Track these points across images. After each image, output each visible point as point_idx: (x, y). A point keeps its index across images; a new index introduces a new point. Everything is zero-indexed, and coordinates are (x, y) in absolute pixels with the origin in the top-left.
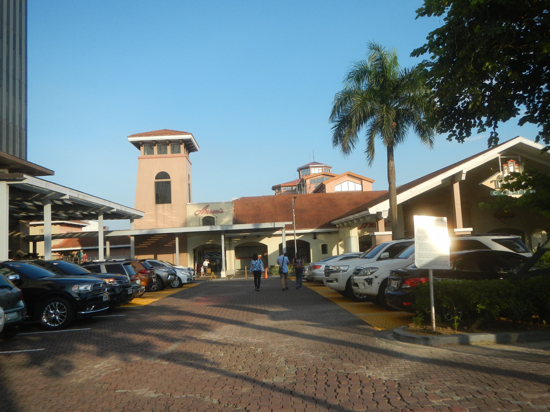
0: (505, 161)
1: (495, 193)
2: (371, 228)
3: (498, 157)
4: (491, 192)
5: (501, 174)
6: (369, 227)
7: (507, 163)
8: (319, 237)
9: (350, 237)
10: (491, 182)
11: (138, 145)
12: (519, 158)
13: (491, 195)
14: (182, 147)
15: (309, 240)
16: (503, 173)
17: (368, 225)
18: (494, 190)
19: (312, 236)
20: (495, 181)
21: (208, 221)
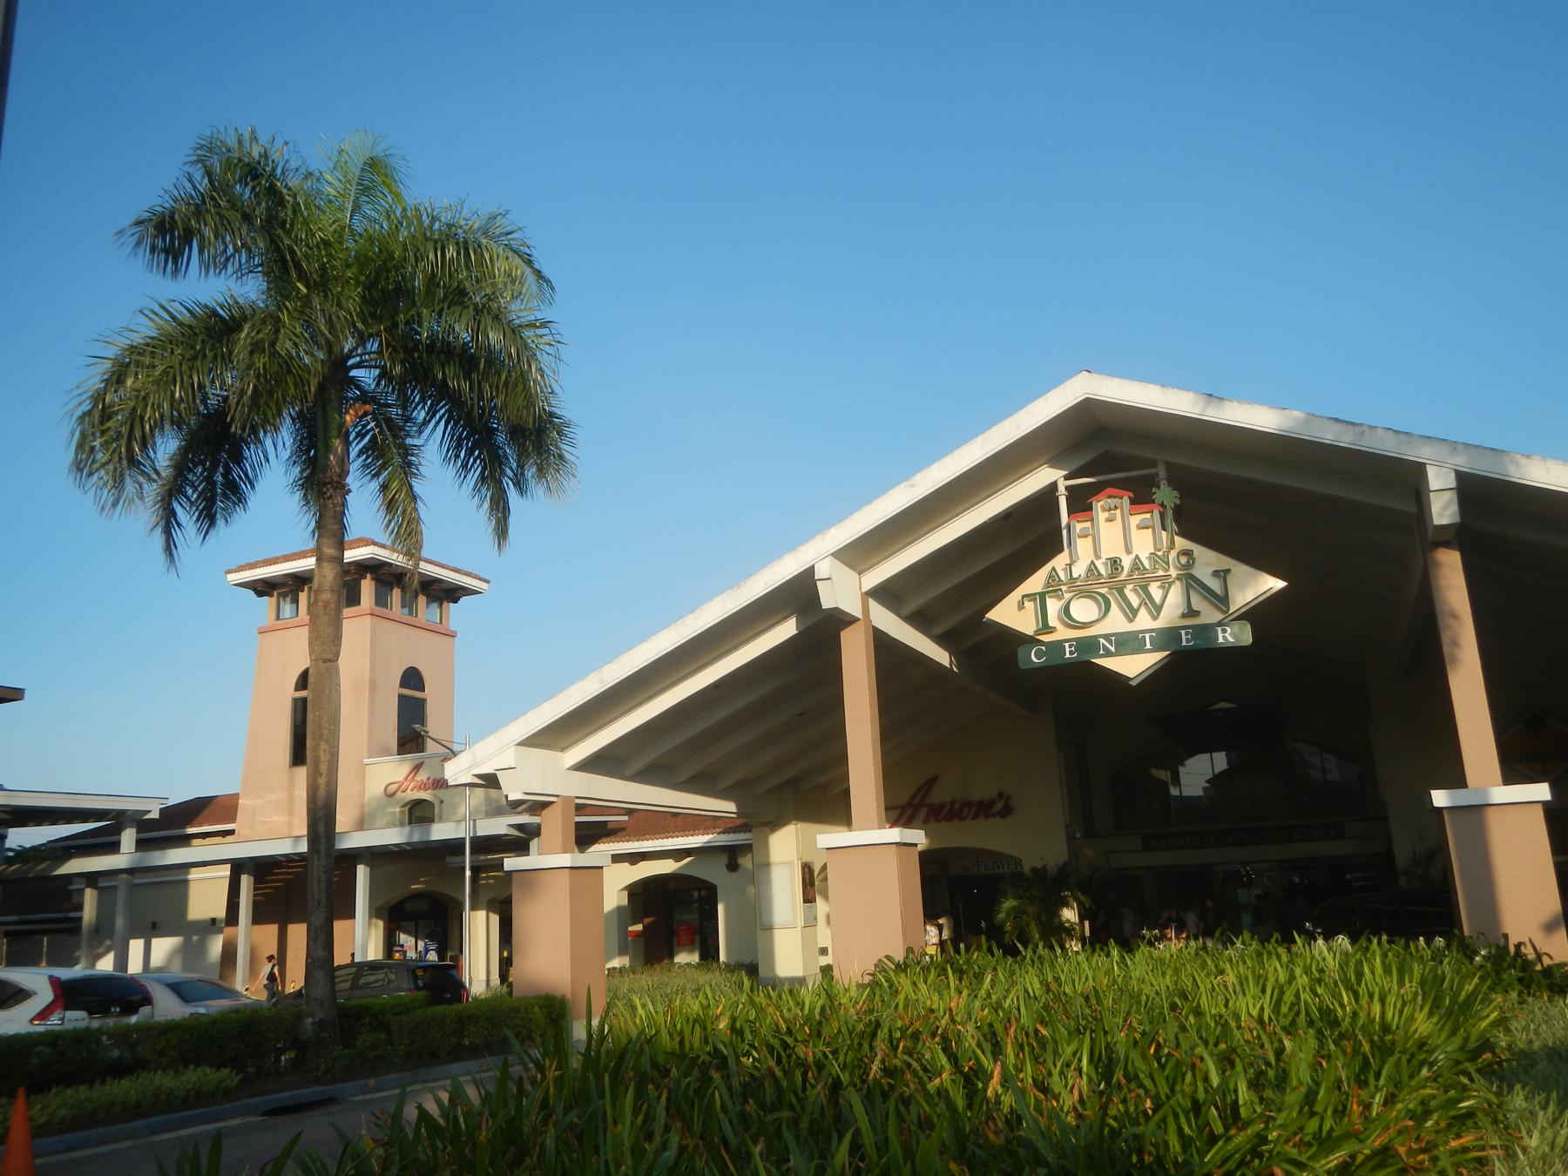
0: (1081, 502)
2: (933, 824)
4: (1021, 651)
5: (1059, 562)
8: (745, 862)
9: (767, 865)
10: (1021, 606)
11: (263, 588)
13: (1023, 666)
14: (367, 587)
15: (713, 872)
17: (923, 812)
18: (1031, 641)
19: (723, 860)
21: (419, 813)
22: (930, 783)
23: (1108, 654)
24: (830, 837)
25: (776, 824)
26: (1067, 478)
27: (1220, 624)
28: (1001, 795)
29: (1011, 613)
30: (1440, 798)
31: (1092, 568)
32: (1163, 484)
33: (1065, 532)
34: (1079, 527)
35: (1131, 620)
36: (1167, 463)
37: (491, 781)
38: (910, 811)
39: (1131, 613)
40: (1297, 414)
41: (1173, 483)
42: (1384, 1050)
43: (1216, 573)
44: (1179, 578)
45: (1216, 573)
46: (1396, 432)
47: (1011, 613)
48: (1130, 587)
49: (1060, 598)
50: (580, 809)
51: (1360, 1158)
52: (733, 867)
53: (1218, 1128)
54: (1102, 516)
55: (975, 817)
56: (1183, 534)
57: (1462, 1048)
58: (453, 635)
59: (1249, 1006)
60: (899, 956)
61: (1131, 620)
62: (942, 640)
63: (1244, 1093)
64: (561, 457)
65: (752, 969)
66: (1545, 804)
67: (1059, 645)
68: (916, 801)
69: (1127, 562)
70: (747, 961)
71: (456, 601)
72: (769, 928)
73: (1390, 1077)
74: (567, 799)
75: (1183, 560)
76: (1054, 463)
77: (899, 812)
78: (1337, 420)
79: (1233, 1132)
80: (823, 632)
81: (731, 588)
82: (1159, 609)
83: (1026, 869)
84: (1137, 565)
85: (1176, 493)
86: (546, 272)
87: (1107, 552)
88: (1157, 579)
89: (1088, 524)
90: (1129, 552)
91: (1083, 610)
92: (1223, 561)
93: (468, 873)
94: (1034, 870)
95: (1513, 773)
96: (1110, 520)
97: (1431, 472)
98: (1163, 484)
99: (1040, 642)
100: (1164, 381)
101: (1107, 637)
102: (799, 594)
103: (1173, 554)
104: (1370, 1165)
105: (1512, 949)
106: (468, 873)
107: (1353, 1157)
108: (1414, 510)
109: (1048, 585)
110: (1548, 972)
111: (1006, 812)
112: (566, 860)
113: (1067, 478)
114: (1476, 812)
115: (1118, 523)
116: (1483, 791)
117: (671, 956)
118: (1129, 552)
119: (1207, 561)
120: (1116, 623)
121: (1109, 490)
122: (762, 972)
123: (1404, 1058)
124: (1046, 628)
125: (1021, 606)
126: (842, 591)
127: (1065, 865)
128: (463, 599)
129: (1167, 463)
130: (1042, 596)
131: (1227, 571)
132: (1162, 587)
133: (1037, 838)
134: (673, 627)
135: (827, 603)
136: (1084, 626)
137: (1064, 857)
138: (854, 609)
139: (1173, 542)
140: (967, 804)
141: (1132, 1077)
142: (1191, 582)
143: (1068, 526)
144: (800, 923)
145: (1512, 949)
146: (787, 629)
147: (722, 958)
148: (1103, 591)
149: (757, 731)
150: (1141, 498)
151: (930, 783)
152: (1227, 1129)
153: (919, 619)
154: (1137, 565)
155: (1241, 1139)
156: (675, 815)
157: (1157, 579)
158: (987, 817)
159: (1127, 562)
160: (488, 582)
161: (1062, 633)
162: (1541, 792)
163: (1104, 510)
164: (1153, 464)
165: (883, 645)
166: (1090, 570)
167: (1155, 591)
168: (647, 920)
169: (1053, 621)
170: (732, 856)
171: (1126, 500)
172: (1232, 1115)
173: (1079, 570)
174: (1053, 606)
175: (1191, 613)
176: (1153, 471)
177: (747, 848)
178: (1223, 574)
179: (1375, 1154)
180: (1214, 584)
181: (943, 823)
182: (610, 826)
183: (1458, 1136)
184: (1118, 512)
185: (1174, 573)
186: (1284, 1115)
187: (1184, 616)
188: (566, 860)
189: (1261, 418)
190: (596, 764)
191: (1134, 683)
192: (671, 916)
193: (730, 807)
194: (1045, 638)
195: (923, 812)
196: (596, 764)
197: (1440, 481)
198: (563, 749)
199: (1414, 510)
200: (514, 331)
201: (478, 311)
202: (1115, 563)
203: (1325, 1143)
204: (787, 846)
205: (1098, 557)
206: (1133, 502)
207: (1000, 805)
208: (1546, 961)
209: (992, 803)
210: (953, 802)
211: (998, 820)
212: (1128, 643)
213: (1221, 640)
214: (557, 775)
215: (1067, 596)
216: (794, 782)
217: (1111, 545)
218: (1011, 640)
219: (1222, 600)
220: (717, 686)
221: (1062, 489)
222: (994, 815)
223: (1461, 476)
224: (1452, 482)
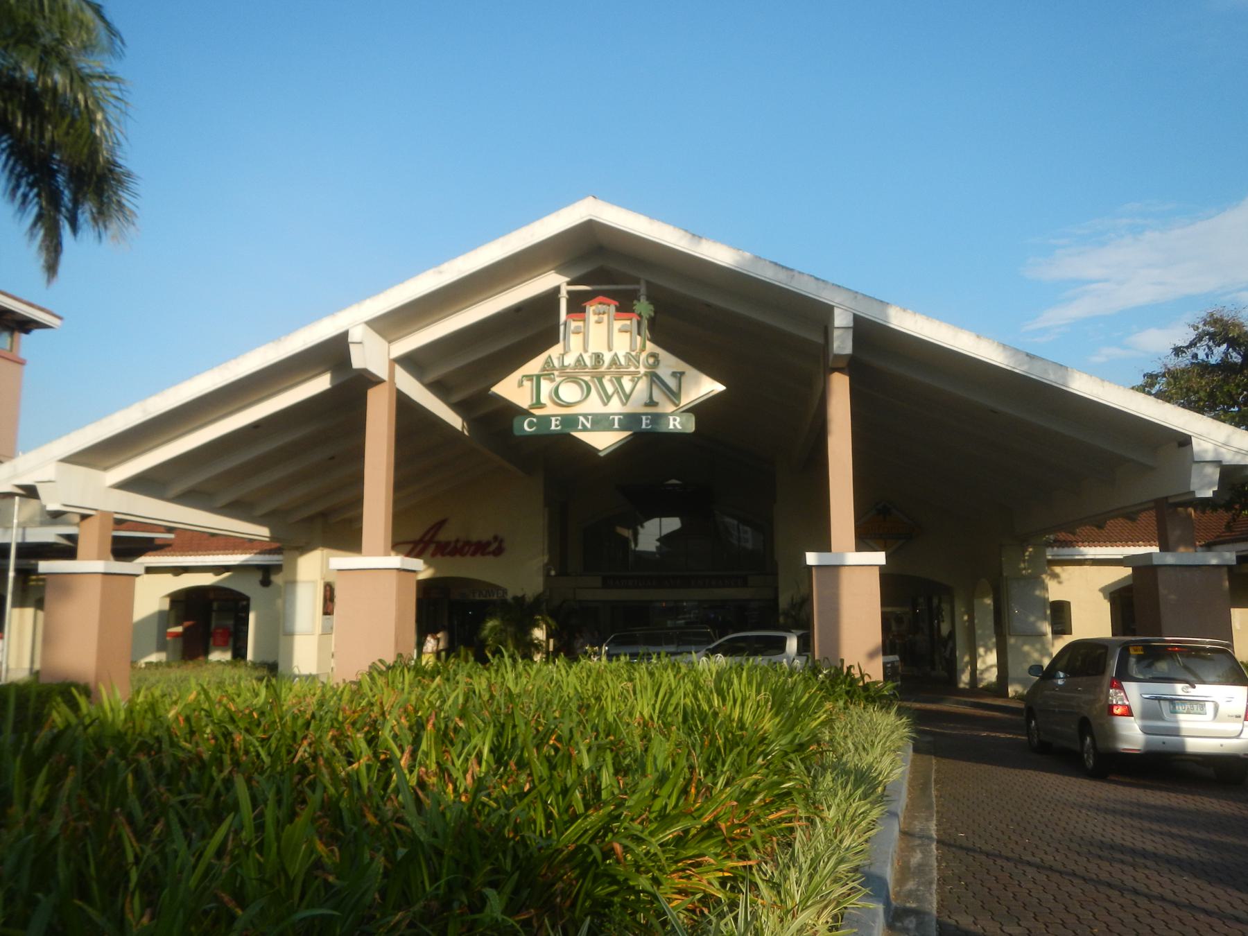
0: (578, 305)
1: (530, 425)
2: (439, 557)
3: (557, 290)
4: (516, 421)
5: (555, 352)
6: (433, 555)
7: (583, 310)
8: (277, 579)
9: (292, 583)
10: (520, 384)
12: (643, 290)
13: (517, 433)
16: (566, 351)
17: (432, 548)
18: (526, 413)
19: (259, 576)
20: (529, 377)
22: (440, 525)
23: (585, 429)
24: (342, 561)
25: (304, 549)
26: (569, 284)
27: (672, 413)
28: (496, 538)
29: (512, 389)
30: (812, 558)
31: (580, 360)
32: (643, 299)
33: (562, 328)
34: (573, 325)
35: (605, 404)
36: (648, 283)
37: (30, 492)
38: (421, 546)
39: (606, 399)
40: (747, 255)
41: (650, 298)
42: (732, 744)
43: (674, 374)
44: (646, 374)
45: (674, 374)
46: (817, 279)
47: (512, 389)
48: (608, 377)
49: (552, 380)
50: (119, 523)
51: (693, 831)
52: (266, 582)
53: (580, 808)
54: (592, 318)
55: (473, 554)
56: (654, 340)
57: (792, 741)
58: (21, 363)
59: (644, 707)
60: (390, 660)
61: (605, 404)
62: (457, 407)
63: (606, 778)
64: (119, 202)
65: (271, 669)
66: (881, 567)
67: (546, 420)
68: (427, 538)
69: (607, 357)
70: (270, 660)
71: (27, 331)
72: (290, 634)
73: (733, 764)
74: (105, 514)
75: (651, 361)
76: (560, 270)
77: (399, 544)
78: (776, 264)
79: (590, 812)
80: (353, 388)
81: (273, 341)
82: (628, 397)
83: (509, 597)
84: (615, 361)
85: (651, 307)
86: (118, 25)
87: (593, 348)
88: (629, 373)
89: (581, 324)
90: (610, 349)
91: (570, 392)
92: (680, 365)
93: (11, 574)
94: (515, 598)
95: (864, 541)
96: (598, 322)
97: (837, 312)
98: (643, 299)
99: (532, 415)
100: (653, 215)
101: (585, 416)
102: (333, 353)
103: (644, 355)
104: (699, 838)
105: (845, 670)
106: (11, 574)
107: (686, 831)
108: (821, 341)
109: (544, 369)
110: (866, 687)
111: (498, 552)
112: (99, 566)
113: (569, 284)
114: (833, 571)
115: (604, 326)
116: (841, 555)
117: (206, 653)
118: (610, 349)
119: (669, 363)
120: (594, 405)
121: (600, 298)
122: (281, 668)
123: (746, 751)
124: (538, 404)
125: (520, 384)
126: (371, 355)
127: (540, 595)
128: (36, 333)
129: (648, 283)
130: (538, 377)
131: (682, 374)
132: (632, 380)
133: (523, 573)
134: (216, 370)
135: (357, 363)
136: (569, 405)
137: (540, 589)
138: (379, 368)
139: (643, 348)
140: (468, 543)
141: (522, 764)
142: (654, 378)
143: (565, 324)
144: (318, 630)
145: (845, 670)
146: (321, 383)
147: (250, 656)
148: (587, 378)
149: (290, 466)
150: (625, 306)
151: (440, 525)
152: (587, 807)
153: (439, 388)
154: (615, 361)
155: (595, 817)
156: (213, 535)
157: (629, 373)
158: (483, 554)
159: (607, 357)
160: (60, 318)
161: (550, 409)
162: (879, 558)
163: (595, 314)
164: (637, 281)
165: (404, 404)
166: (578, 361)
167: (627, 383)
168: (187, 624)
169: (544, 398)
170: (266, 574)
171: (613, 308)
172: (594, 796)
173: (570, 360)
174: (546, 387)
175: (651, 403)
176: (636, 287)
177: (278, 568)
178: (678, 375)
179: (703, 829)
180: (672, 383)
181: (448, 558)
182: (157, 542)
183: (778, 810)
184: (605, 317)
185: (642, 370)
186: (635, 797)
187: (646, 405)
188: (99, 566)
189: (720, 254)
190: (135, 484)
191: (602, 454)
192: (207, 619)
193: (262, 532)
194: (537, 412)
195: (432, 548)
196: (135, 484)
197: (841, 319)
198: (105, 469)
199: (821, 341)
200: (81, 79)
201: (46, 52)
202: (598, 357)
203: (664, 819)
204: (313, 568)
205: (586, 351)
206: (618, 309)
207: (494, 546)
208: (867, 680)
209: (488, 544)
210: (457, 541)
211: (490, 558)
212: (601, 422)
213: (671, 427)
214: (102, 492)
215: (558, 380)
216: (324, 515)
217: (597, 343)
218: (511, 411)
219: (674, 395)
220: (256, 426)
221: (564, 290)
222: (489, 553)
223: (856, 318)
224: (851, 325)
